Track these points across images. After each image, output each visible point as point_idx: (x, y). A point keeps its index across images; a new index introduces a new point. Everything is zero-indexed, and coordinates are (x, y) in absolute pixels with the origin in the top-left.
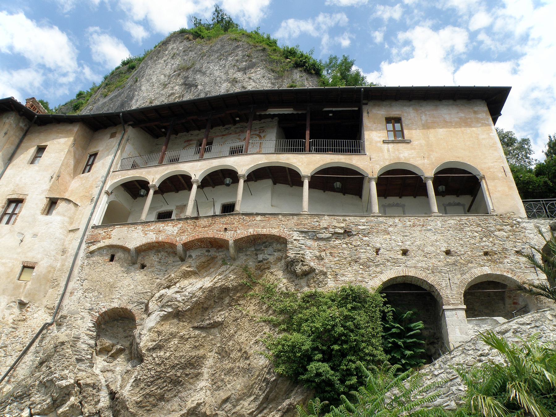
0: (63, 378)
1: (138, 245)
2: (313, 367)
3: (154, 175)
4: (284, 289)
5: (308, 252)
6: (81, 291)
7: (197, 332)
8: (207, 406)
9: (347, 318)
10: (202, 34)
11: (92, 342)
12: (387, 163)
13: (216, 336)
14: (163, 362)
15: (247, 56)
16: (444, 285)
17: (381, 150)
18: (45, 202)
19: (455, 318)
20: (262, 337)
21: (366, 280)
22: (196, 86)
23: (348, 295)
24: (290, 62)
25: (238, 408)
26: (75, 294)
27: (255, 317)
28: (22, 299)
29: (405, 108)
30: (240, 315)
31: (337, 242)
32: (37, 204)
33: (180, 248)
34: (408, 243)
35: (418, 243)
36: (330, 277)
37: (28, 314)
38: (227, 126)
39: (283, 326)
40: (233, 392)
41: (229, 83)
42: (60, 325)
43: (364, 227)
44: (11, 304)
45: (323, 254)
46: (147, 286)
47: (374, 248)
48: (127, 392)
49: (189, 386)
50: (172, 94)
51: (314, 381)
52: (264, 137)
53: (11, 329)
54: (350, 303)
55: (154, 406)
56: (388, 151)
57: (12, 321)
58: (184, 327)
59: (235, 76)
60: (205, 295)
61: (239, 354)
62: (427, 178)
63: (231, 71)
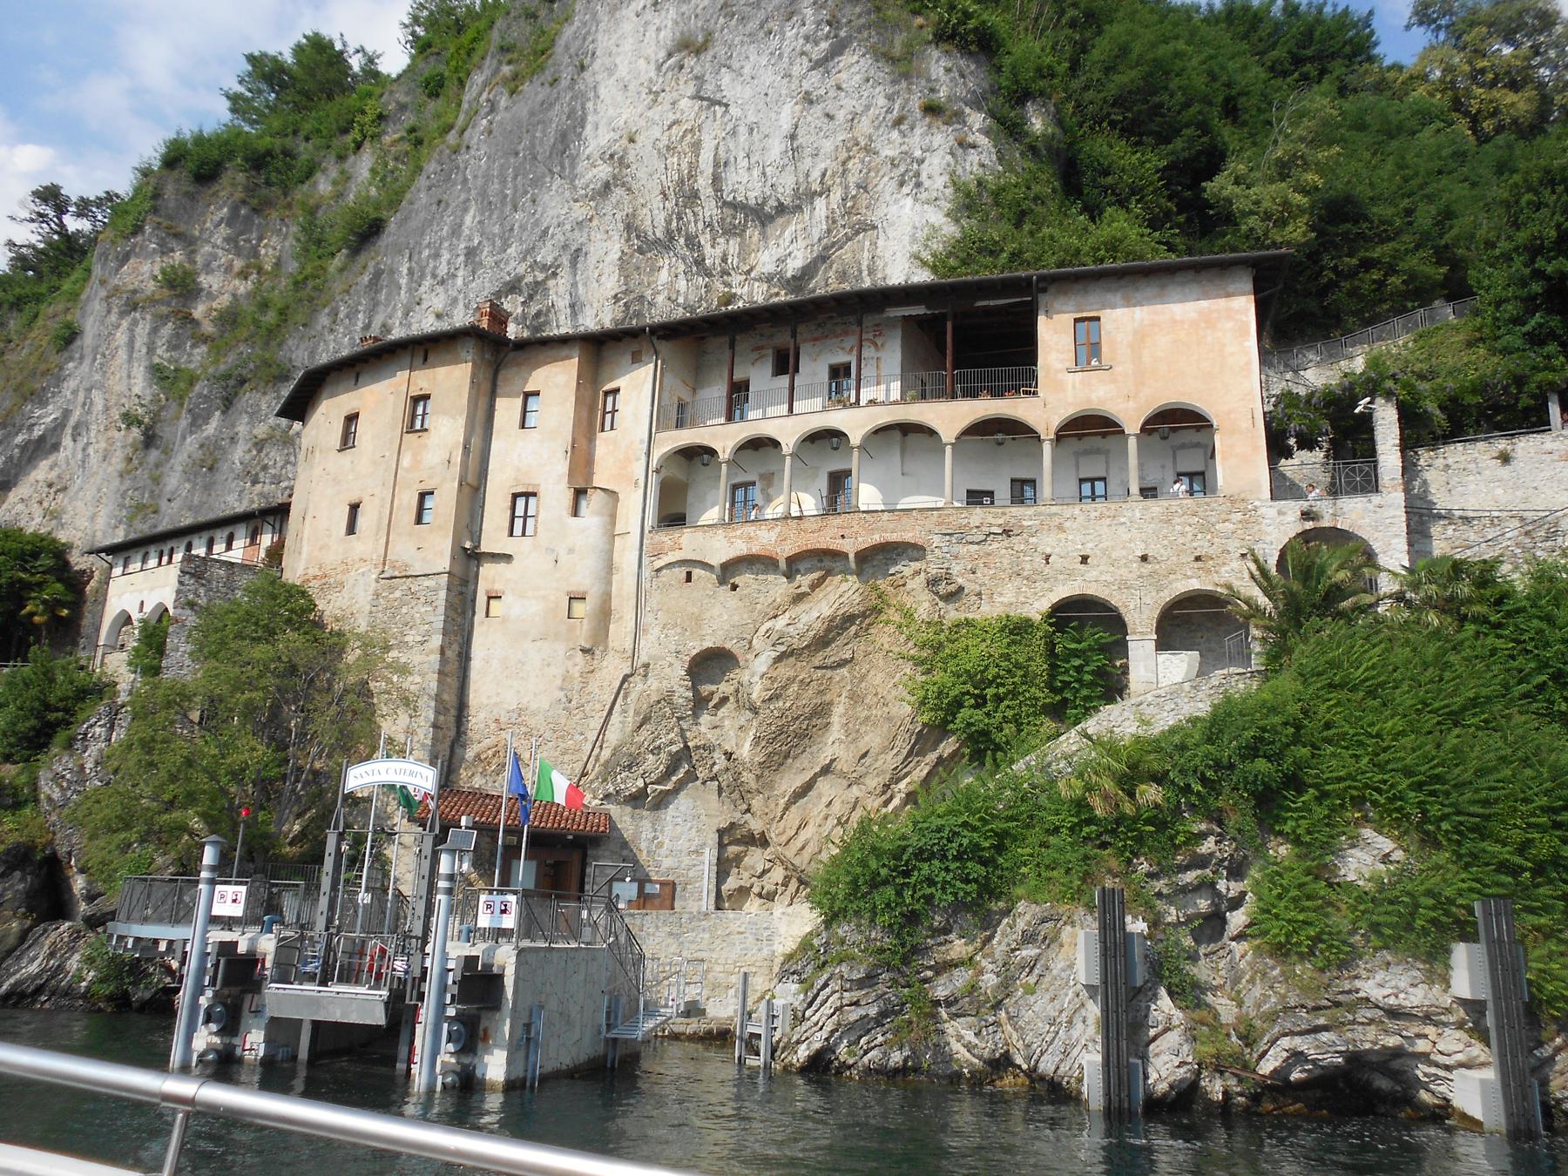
3: (724, 437)
7: (820, 673)
31: (995, 545)
34: (1090, 545)
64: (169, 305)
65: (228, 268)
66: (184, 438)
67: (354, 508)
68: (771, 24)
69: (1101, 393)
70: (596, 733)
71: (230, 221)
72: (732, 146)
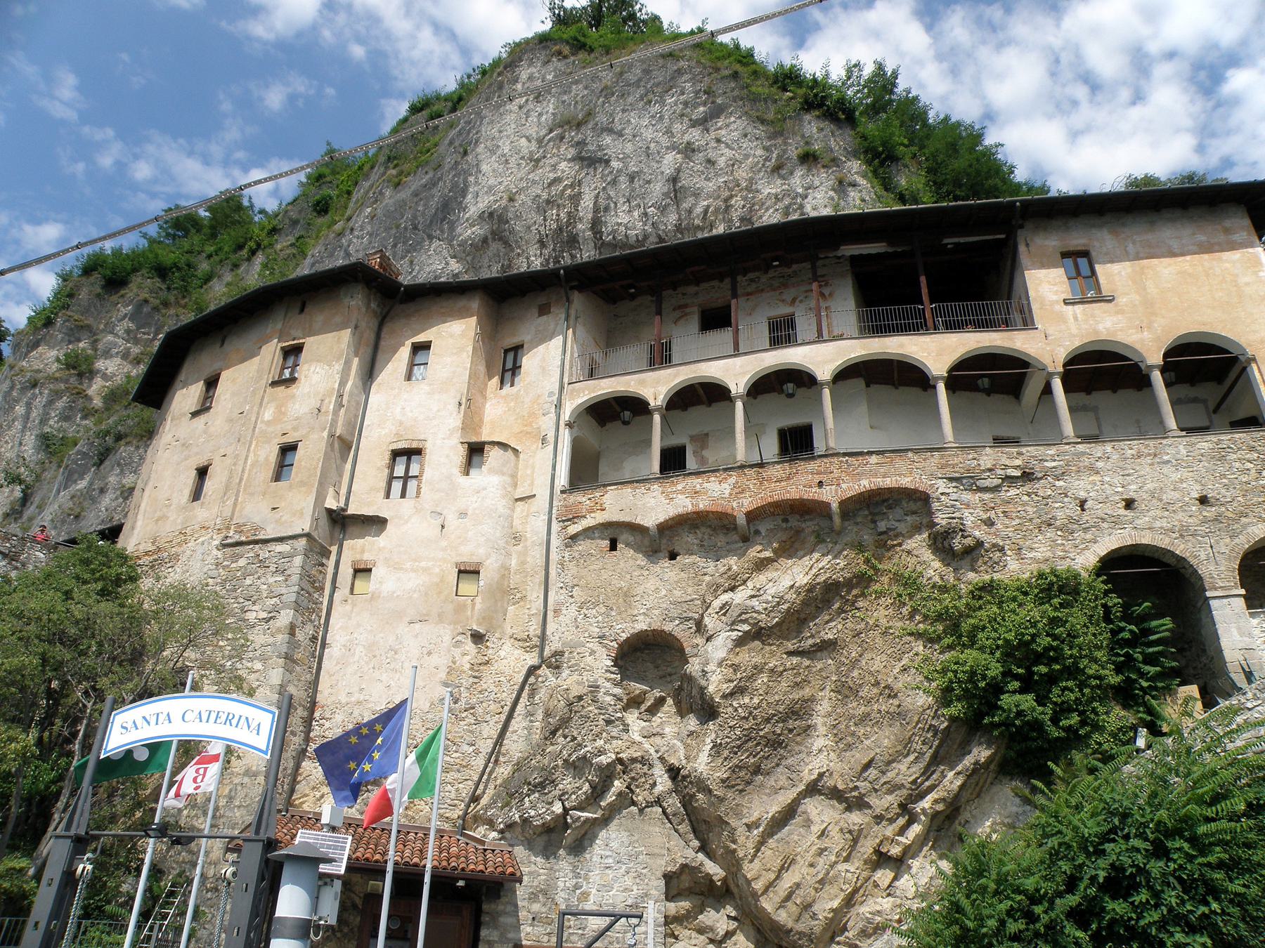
0: (601, 752)
1: (662, 520)
2: (1007, 700)
3: (656, 387)
4: (937, 579)
5: (960, 508)
6: (574, 608)
7: (795, 660)
8: (836, 776)
9: (1054, 622)
10: (589, 42)
11: (617, 691)
12: (1077, 343)
13: (827, 663)
14: (750, 713)
15: (705, 92)
16: (1203, 557)
17: (1062, 318)
18: (462, 451)
19: (1228, 610)
20: (912, 661)
21: (1071, 555)
22: (607, 162)
23: (1051, 584)
24: (792, 98)
25: (890, 775)
26: (564, 612)
27: (890, 628)
28: (475, 628)
29: (1094, 231)
30: (863, 625)
31: (1013, 492)
32: (447, 456)
33: (741, 520)
34: (1133, 487)
35: (1150, 486)
36: (1009, 553)
37: (490, 651)
38: (751, 275)
39: (947, 641)
40: (878, 750)
41: (678, 153)
42: (558, 667)
43: (1054, 464)
44: (459, 638)
45: (992, 514)
46: (690, 590)
47: (1076, 499)
48: (701, 764)
49: (797, 748)
50: (557, 180)
51: (1014, 725)
52: (831, 295)
53: (471, 680)
54: (1056, 596)
55: (748, 783)
56: (1076, 318)
57: (468, 666)
58: (772, 653)
59: (687, 138)
60: (801, 597)
61: (875, 691)
62: (1151, 367)
63: (677, 127)
64: (67, 381)
65: (125, 356)
66: (58, 492)
67: (202, 472)
68: (651, 96)
69: (1108, 324)
70: (490, 743)
71: (133, 317)
72: (612, 193)
